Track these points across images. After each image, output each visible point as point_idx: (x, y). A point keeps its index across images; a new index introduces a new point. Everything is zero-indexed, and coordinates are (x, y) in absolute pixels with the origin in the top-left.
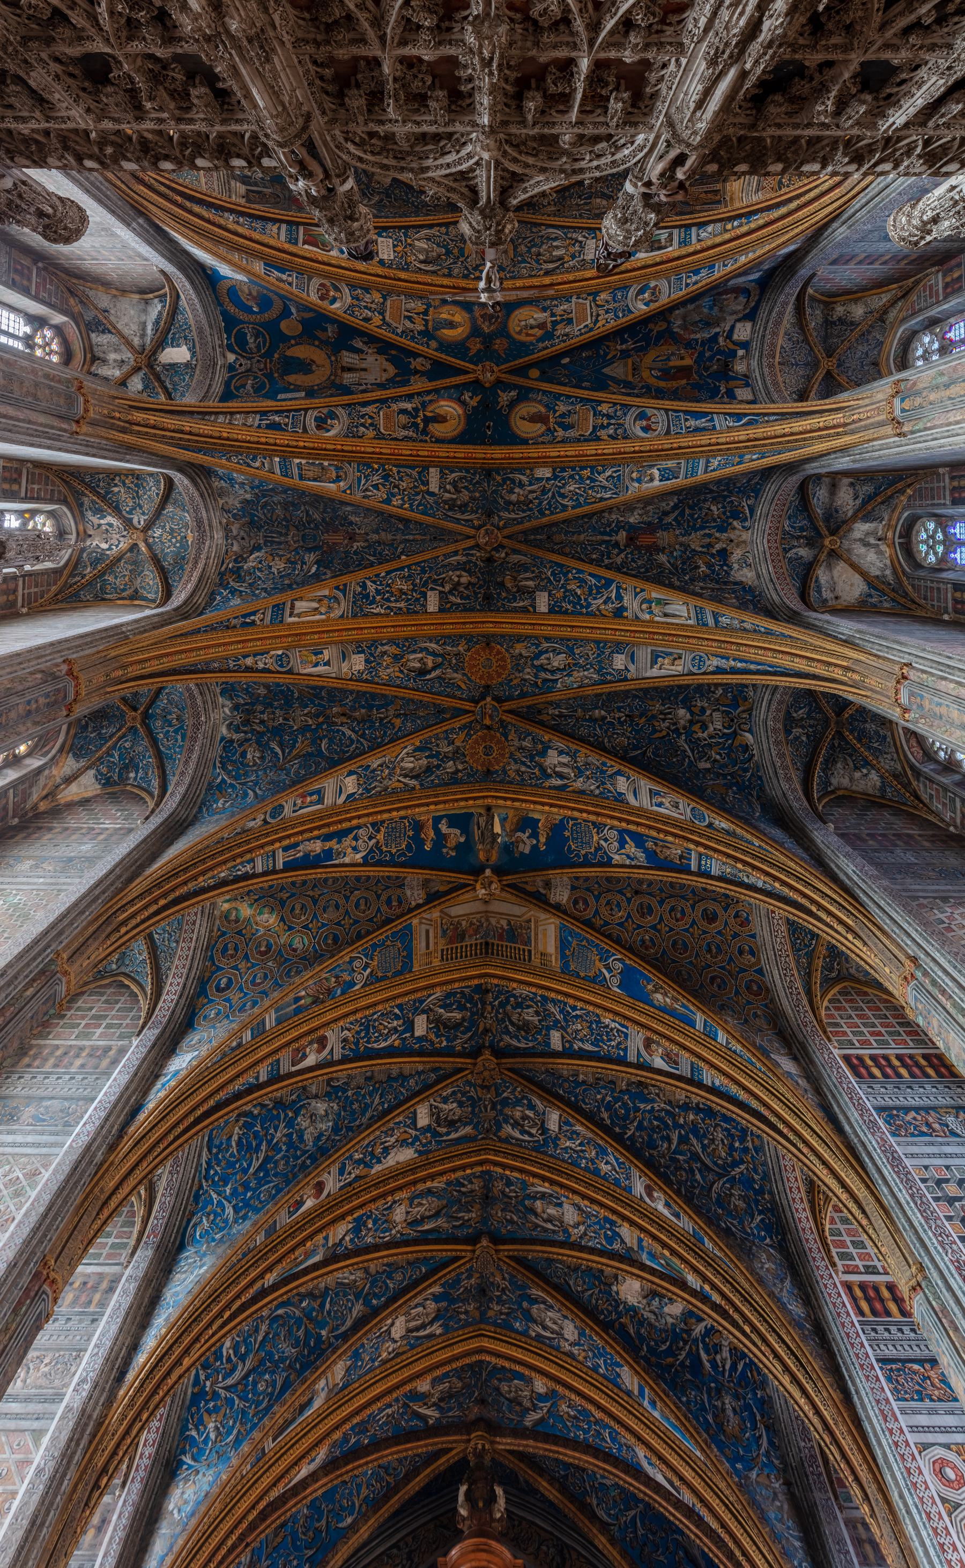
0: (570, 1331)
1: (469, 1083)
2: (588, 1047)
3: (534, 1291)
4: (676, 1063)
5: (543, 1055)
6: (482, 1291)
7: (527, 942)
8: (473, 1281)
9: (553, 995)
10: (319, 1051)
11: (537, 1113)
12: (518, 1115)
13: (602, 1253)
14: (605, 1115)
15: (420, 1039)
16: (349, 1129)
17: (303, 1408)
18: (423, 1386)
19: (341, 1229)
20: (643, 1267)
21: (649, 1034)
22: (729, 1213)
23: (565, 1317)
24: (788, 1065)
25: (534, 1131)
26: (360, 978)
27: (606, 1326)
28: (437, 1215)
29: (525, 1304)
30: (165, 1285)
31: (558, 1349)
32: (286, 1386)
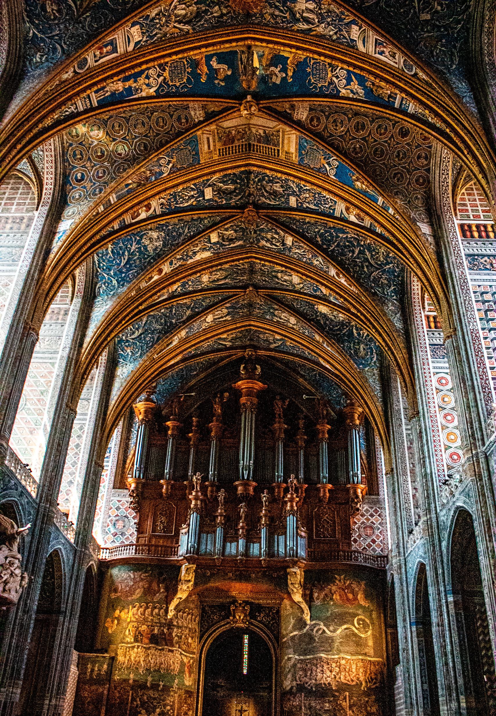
0: (293, 320)
1: (241, 222)
2: (312, 206)
4: (363, 220)
5: (284, 209)
6: (251, 305)
7: (277, 145)
9: (292, 178)
10: (147, 211)
12: (269, 236)
13: (310, 296)
14: (319, 239)
15: (209, 200)
16: (173, 245)
17: (168, 345)
18: (224, 336)
19: (175, 287)
20: (330, 302)
21: (348, 205)
22: (378, 286)
24: (425, 229)
25: (278, 244)
26: (166, 171)
27: (309, 320)
28: (225, 278)
29: (271, 311)
30: (91, 312)
31: (287, 326)
32: (159, 339)
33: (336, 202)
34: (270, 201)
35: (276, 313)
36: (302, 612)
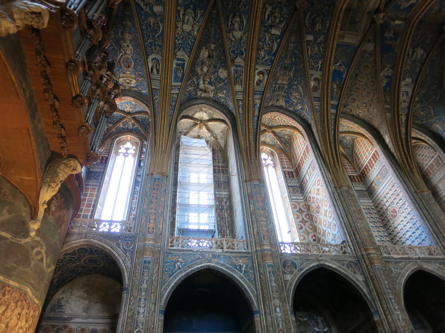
3: (199, 12)
11: (278, 24)
12: (276, 14)
23: (193, 27)
25: (270, 21)
29: (192, 6)
33: (317, 70)
34: (308, 20)
35: (190, 11)
36: (33, 216)
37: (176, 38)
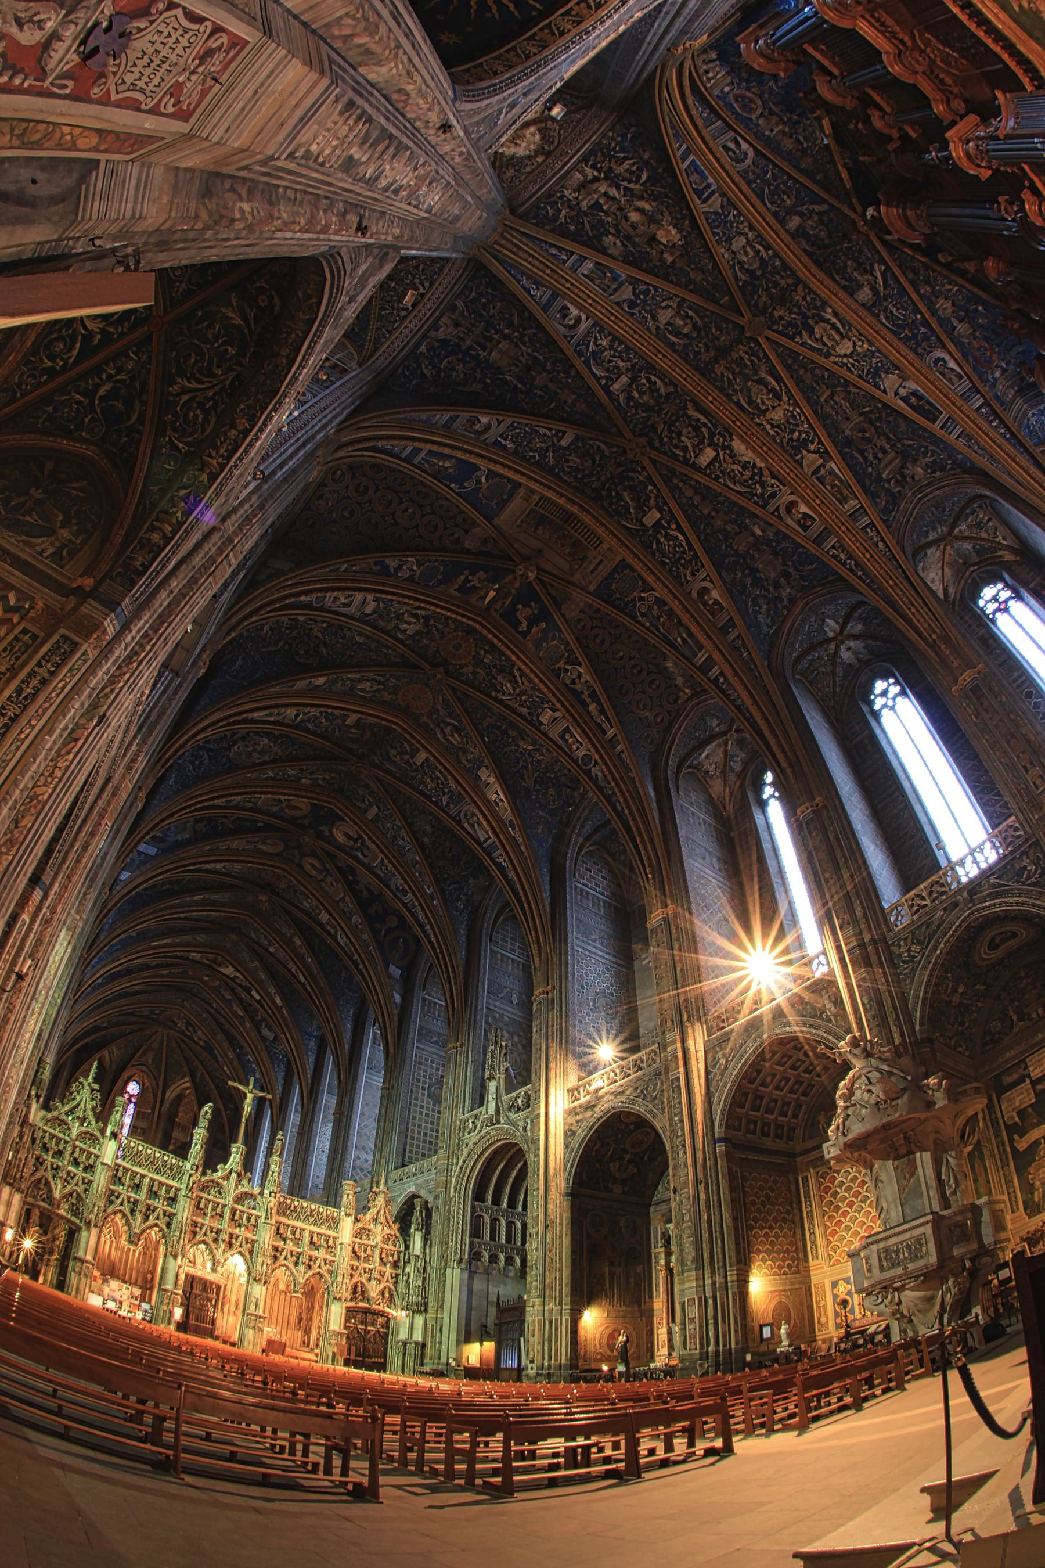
8: (781, 313)
15: (660, 510)
23: (734, 253)
28: (761, 382)
29: (759, 273)
37: (740, 214)
